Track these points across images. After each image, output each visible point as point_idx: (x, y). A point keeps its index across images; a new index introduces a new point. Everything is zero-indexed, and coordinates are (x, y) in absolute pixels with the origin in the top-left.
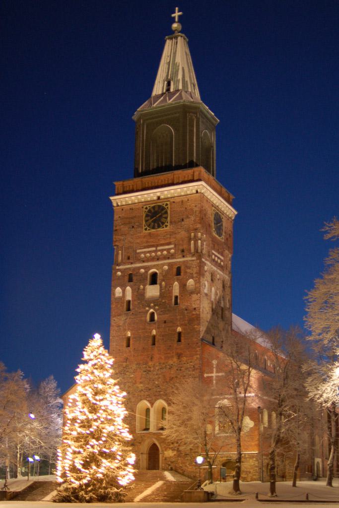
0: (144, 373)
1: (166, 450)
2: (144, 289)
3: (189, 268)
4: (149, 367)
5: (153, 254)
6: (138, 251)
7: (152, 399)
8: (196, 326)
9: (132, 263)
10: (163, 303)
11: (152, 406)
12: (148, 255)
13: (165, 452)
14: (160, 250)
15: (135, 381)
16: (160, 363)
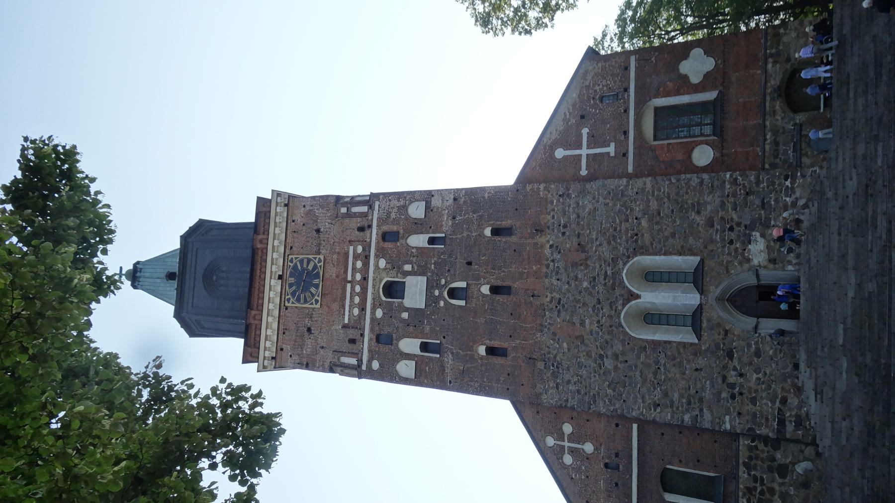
0: (563, 314)
1: (749, 260)
2: (407, 310)
3: (389, 213)
4: (551, 302)
5: (358, 289)
6: (346, 321)
7: (622, 295)
8: (486, 195)
9: (362, 335)
10: (435, 268)
11: (638, 297)
12: (357, 300)
13: (755, 262)
14: (353, 275)
15: (577, 338)
16: (546, 277)
